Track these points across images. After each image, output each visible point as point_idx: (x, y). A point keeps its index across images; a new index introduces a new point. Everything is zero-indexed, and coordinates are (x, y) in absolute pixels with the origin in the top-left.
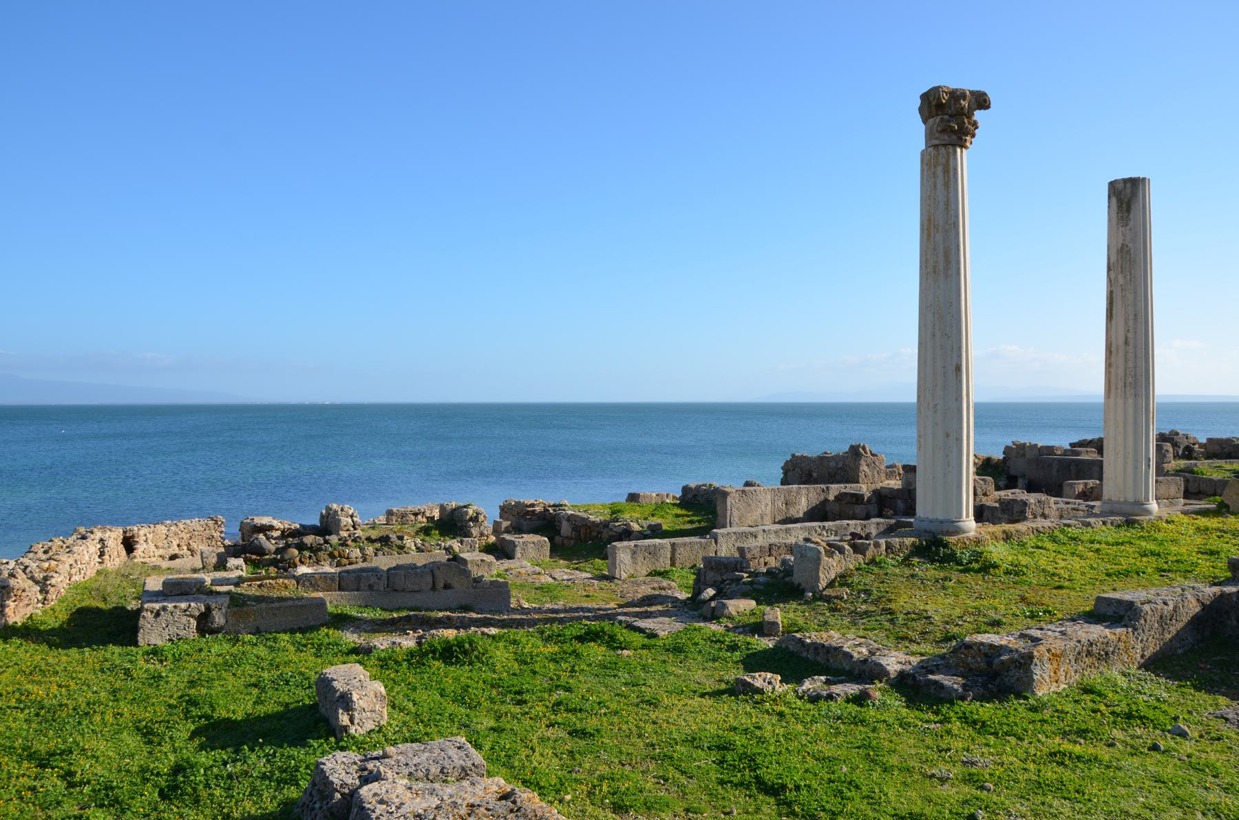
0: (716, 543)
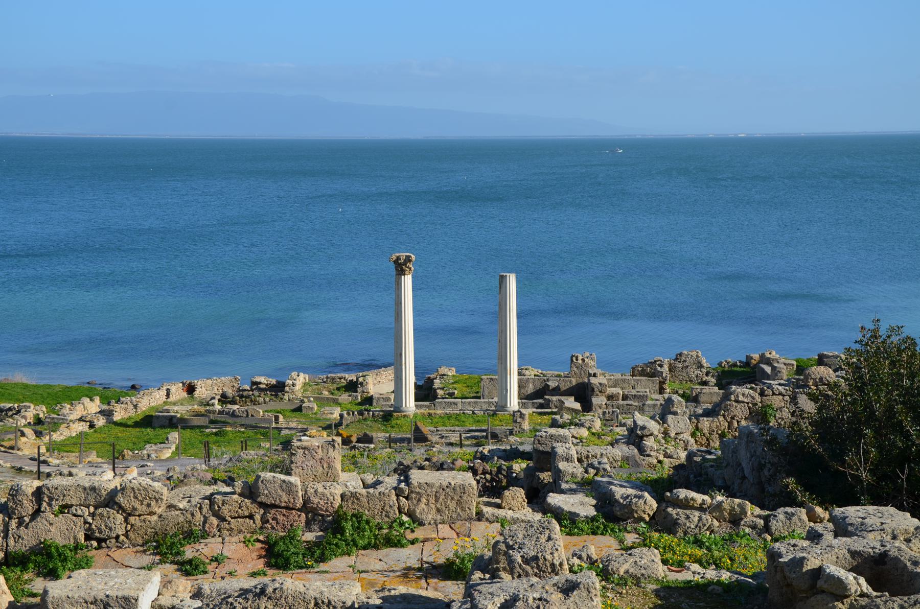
0: (434, 406)
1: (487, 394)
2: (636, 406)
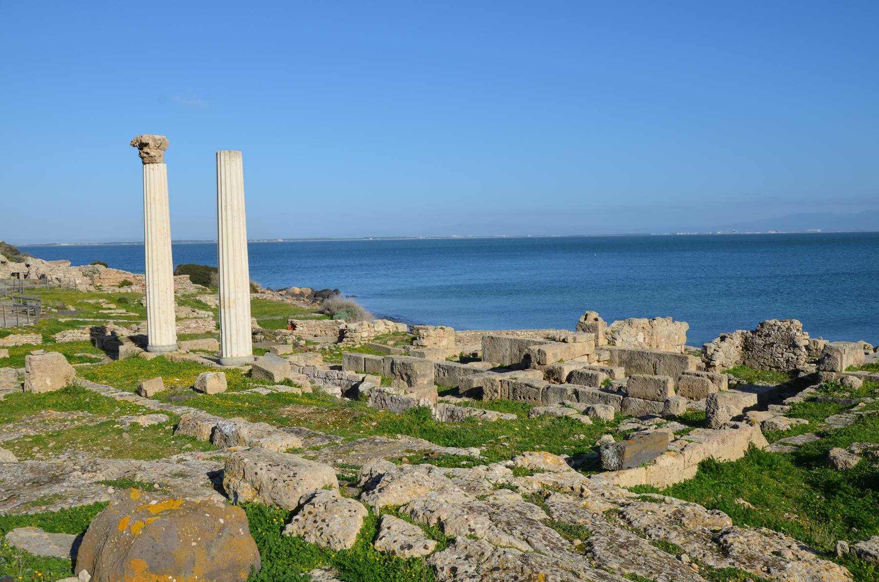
1: (487, 356)
2: (538, 389)
